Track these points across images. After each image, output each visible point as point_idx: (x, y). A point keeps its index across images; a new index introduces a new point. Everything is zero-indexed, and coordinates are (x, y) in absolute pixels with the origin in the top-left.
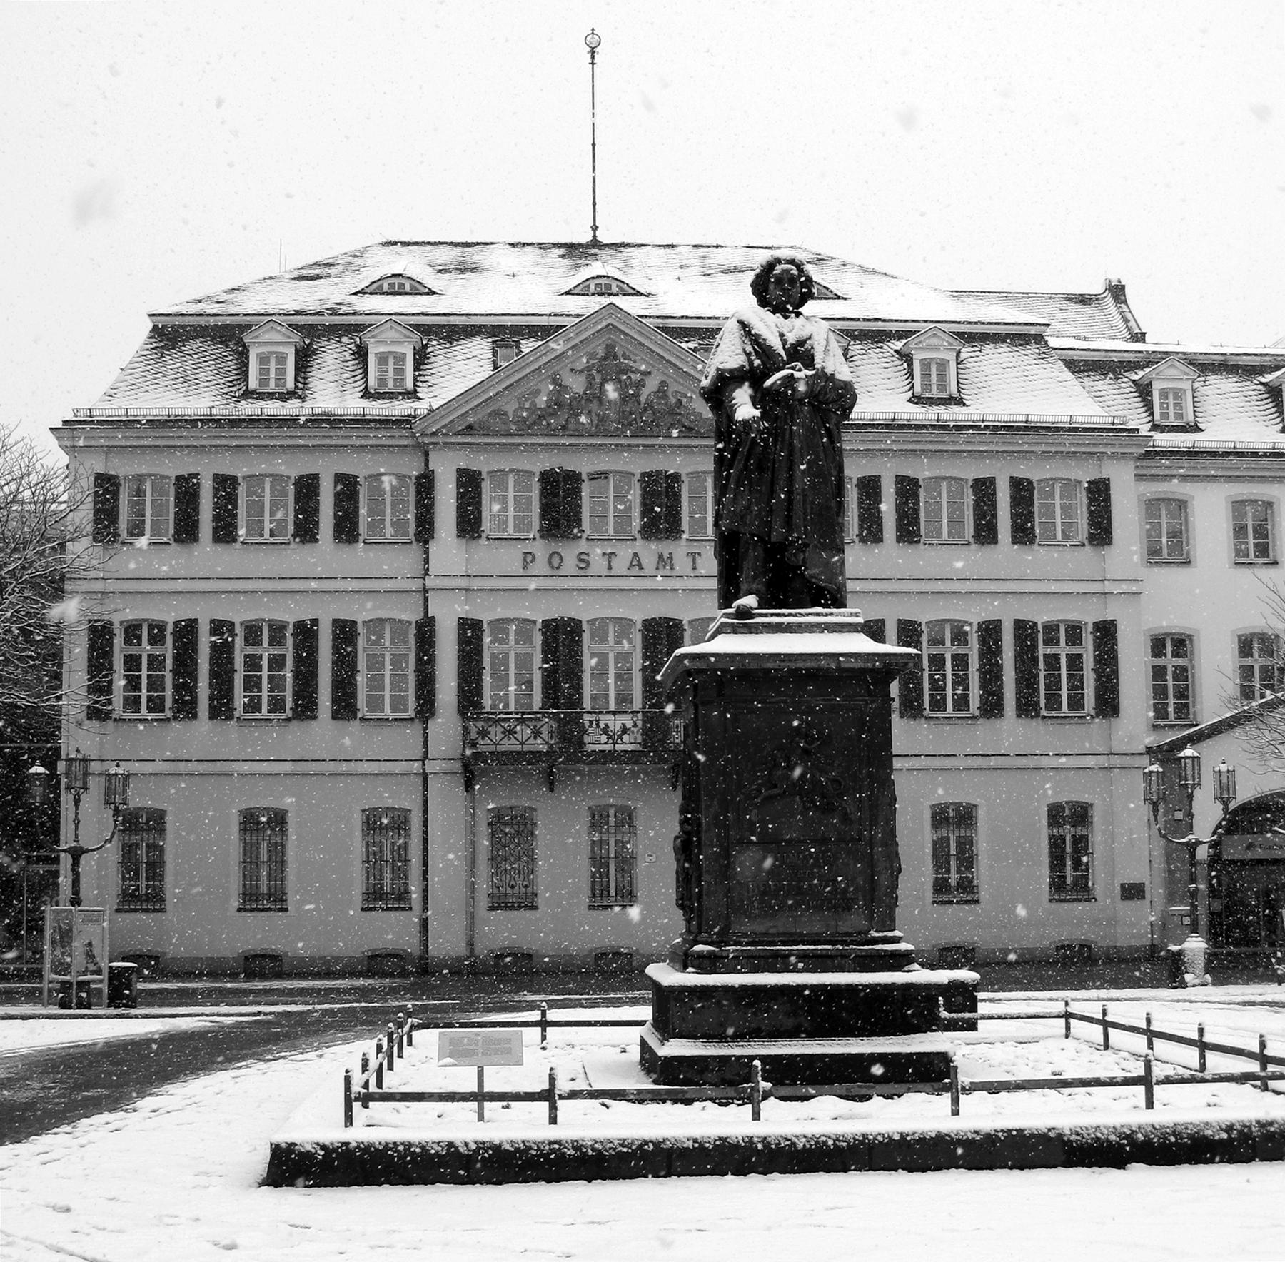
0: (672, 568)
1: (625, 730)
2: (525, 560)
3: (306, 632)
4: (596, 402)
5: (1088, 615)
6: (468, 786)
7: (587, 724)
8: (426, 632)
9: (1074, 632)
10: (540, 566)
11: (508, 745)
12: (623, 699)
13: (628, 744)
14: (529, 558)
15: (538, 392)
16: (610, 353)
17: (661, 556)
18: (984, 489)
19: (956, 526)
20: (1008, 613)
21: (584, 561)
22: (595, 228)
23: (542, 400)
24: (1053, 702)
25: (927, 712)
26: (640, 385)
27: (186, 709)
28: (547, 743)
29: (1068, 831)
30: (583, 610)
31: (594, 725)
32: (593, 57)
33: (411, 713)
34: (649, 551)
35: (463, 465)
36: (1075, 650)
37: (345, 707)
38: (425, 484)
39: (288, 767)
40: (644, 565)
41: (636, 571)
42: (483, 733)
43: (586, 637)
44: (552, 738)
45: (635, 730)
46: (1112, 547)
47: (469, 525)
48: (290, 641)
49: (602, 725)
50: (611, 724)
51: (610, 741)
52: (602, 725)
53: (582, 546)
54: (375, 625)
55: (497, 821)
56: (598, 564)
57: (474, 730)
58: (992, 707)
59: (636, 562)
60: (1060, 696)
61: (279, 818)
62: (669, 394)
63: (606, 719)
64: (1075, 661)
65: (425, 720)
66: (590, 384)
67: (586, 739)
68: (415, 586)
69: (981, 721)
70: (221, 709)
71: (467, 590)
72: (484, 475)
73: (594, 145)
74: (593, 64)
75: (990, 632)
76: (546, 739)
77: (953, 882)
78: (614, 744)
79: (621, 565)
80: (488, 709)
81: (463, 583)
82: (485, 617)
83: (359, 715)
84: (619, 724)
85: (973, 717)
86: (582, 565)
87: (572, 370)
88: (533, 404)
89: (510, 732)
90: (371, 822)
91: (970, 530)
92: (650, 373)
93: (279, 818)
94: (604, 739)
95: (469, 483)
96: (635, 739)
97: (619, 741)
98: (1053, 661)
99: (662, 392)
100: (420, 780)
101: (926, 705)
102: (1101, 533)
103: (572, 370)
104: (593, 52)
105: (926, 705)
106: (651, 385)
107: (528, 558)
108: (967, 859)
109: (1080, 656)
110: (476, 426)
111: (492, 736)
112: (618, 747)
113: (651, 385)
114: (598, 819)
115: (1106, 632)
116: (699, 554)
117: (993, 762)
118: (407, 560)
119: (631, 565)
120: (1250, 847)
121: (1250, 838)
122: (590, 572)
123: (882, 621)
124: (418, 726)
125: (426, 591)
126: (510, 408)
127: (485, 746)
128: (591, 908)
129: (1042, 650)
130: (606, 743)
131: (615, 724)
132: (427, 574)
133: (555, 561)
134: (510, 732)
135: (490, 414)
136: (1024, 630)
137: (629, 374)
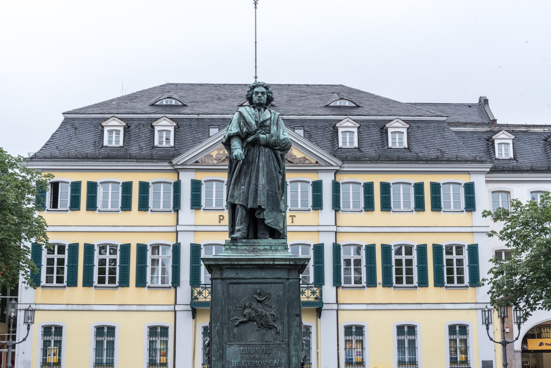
2: (220, 218)
3: (126, 249)
5: (466, 241)
6: (194, 317)
8: (176, 249)
9: (459, 249)
14: (222, 218)
18: (419, 188)
19: (407, 204)
20: (430, 241)
22: (256, 77)
24: (450, 280)
27: (72, 283)
29: (458, 338)
32: (256, 5)
33: (170, 285)
36: (459, 257)
37: (141, 282)
38: (177, 186)
39: (116, 308)
42: (200, 293)
46: (476, 212)
47: (196, 204)
48: (118, 252)
54: (156, 248)
57: (196, 292)
58: (423, 283)
60: (402, 277)
61: (111, 330)
64: (460, 262)
65: (176, 288)
68: (173, 229)
69: (418, 288)
70: (88, 282)
71: (195, 231)
72: (203, 182)
73: (256, 42)
74: (256, 8)
75: (422, 249)
77: (407, 360)
80: (203, 283)
81: (193, 228)
82: (202, 243)
83: (147, 285)
85: (416, 287)
90: (153, 331)
91: (413, 205)
93: (111, 330)
95: (196, 186)
98: (450, 262)
100: (173, 313)
101: (394, 280)
102: (470, 205)
104: (256, 4)
109: (462, 260)
111: (204, 294)
115: (473, 250)
116: (295, 216)
117: (424, 307)
118: (170, 218)
120: (541, 344)
121: (540, 340)
123: (375, 245)
124: (173, 290)
125: (177, 232)
129: (445, 257)
132: (177, 224)
136: (437, 249)
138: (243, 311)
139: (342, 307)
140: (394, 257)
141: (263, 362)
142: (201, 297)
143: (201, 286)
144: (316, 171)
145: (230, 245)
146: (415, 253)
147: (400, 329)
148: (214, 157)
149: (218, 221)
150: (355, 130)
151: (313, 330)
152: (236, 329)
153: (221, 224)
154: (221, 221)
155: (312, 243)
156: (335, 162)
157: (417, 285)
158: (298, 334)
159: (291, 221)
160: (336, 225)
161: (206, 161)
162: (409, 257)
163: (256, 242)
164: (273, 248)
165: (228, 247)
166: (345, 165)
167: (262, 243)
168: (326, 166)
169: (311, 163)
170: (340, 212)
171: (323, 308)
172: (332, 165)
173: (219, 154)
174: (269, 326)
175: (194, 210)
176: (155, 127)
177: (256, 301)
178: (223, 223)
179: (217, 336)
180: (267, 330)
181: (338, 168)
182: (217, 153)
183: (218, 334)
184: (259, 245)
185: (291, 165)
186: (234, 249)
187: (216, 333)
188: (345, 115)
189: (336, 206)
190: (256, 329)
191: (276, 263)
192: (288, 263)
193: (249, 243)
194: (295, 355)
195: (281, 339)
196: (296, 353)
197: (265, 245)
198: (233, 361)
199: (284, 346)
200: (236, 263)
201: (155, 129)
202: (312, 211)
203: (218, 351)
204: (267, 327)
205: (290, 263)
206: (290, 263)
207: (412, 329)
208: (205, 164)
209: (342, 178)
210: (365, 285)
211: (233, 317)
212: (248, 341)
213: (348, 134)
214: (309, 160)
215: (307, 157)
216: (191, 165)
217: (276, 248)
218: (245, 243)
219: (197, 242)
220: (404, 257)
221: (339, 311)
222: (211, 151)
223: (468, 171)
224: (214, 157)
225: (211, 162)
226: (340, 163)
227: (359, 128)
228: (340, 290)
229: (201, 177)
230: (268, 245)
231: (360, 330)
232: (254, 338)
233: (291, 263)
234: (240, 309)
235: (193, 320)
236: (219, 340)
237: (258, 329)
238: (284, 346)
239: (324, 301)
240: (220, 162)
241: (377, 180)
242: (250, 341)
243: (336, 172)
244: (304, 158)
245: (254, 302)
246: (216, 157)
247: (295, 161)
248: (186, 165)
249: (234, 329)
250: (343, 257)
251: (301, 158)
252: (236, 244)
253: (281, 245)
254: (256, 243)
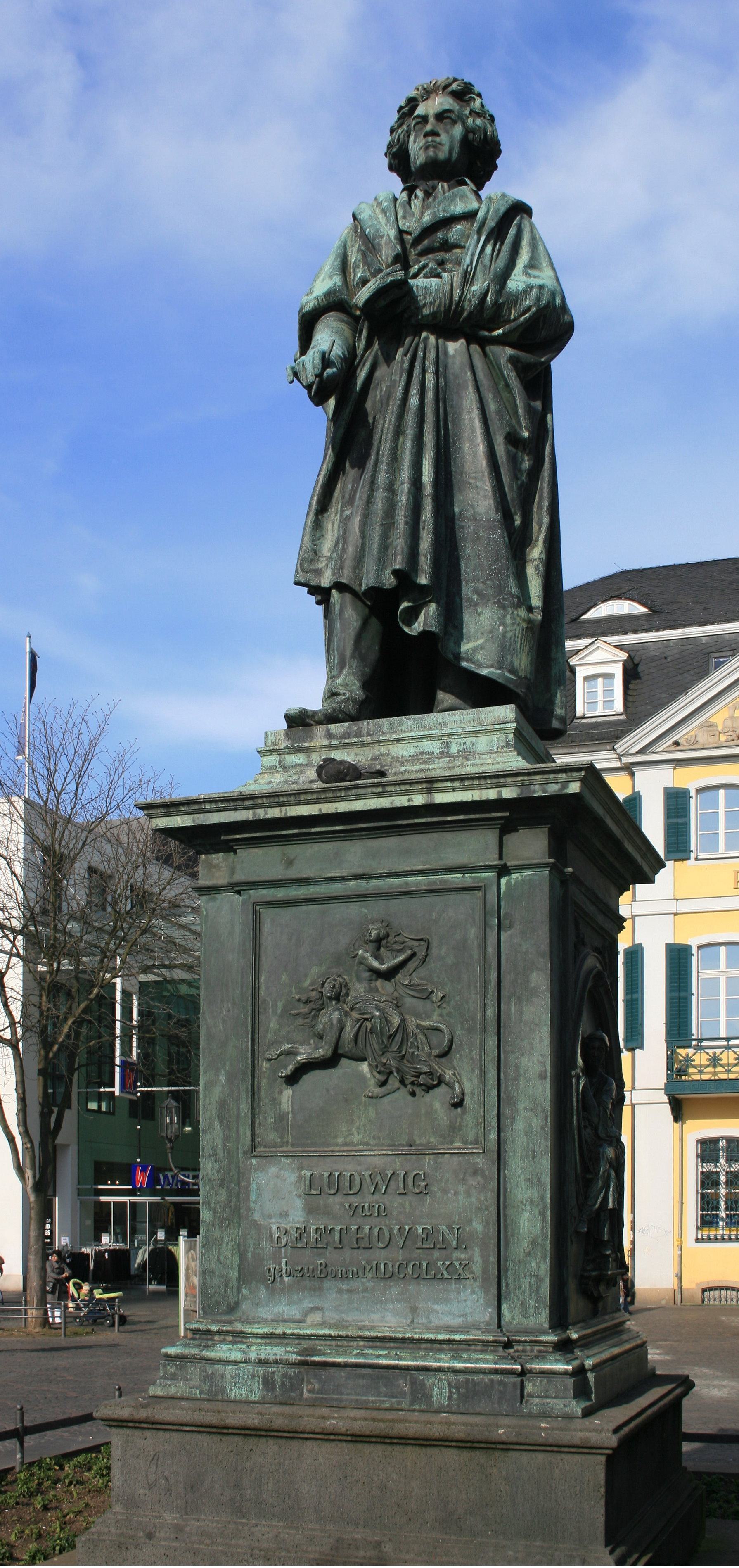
138: (315, 1017)
141: (391, 1230)
145: (279, 752)
148: (720, 728)
152: (288, 1092)
158: (544, 1110)
163: (385, 729)
164: (454, 749)
165: (273, 760)
167: (412, 731)
174: (418, 1077)
176: (578, 669)
177: (367, 974)
179: (217, 1125)
180: (413, 1094)
182: (727, 716)
183: (220, 1117)
184: (398, 741)
186: (296, 765)
187: (215, 1112)
190: (367, 1092)
191: (440, 798)
192: (491, 794)
193: (358, 734)
194: (532, 1202)
195: (471, 1135)
196: (536, 1194)
197: (421, 738)
198: (274, 1228)
199: (480, 1161)
200: (274, 813)
201: (578, 675)
203: (221, 1185)
204: (412, 1083)
205: (499, 793)
206: (499, 793)
211: (277, 1043)
212: (337, 1145)
216: (663, 752)
217: (469, 746)
218: (346, 735)
225: (711, 739)
230: (432, 738)
232: (358, 1128)
233: (508, 793)
234: (304, 1009)
236: (226, 1139)
237: (378, 1091)
238: (480, 1161)
242: (346, 1144)
245: (359, 979)
246: (724, 728)
249: (281, 1092)
252: (306, 745)
253: (486, 732)
254: (384, 733)
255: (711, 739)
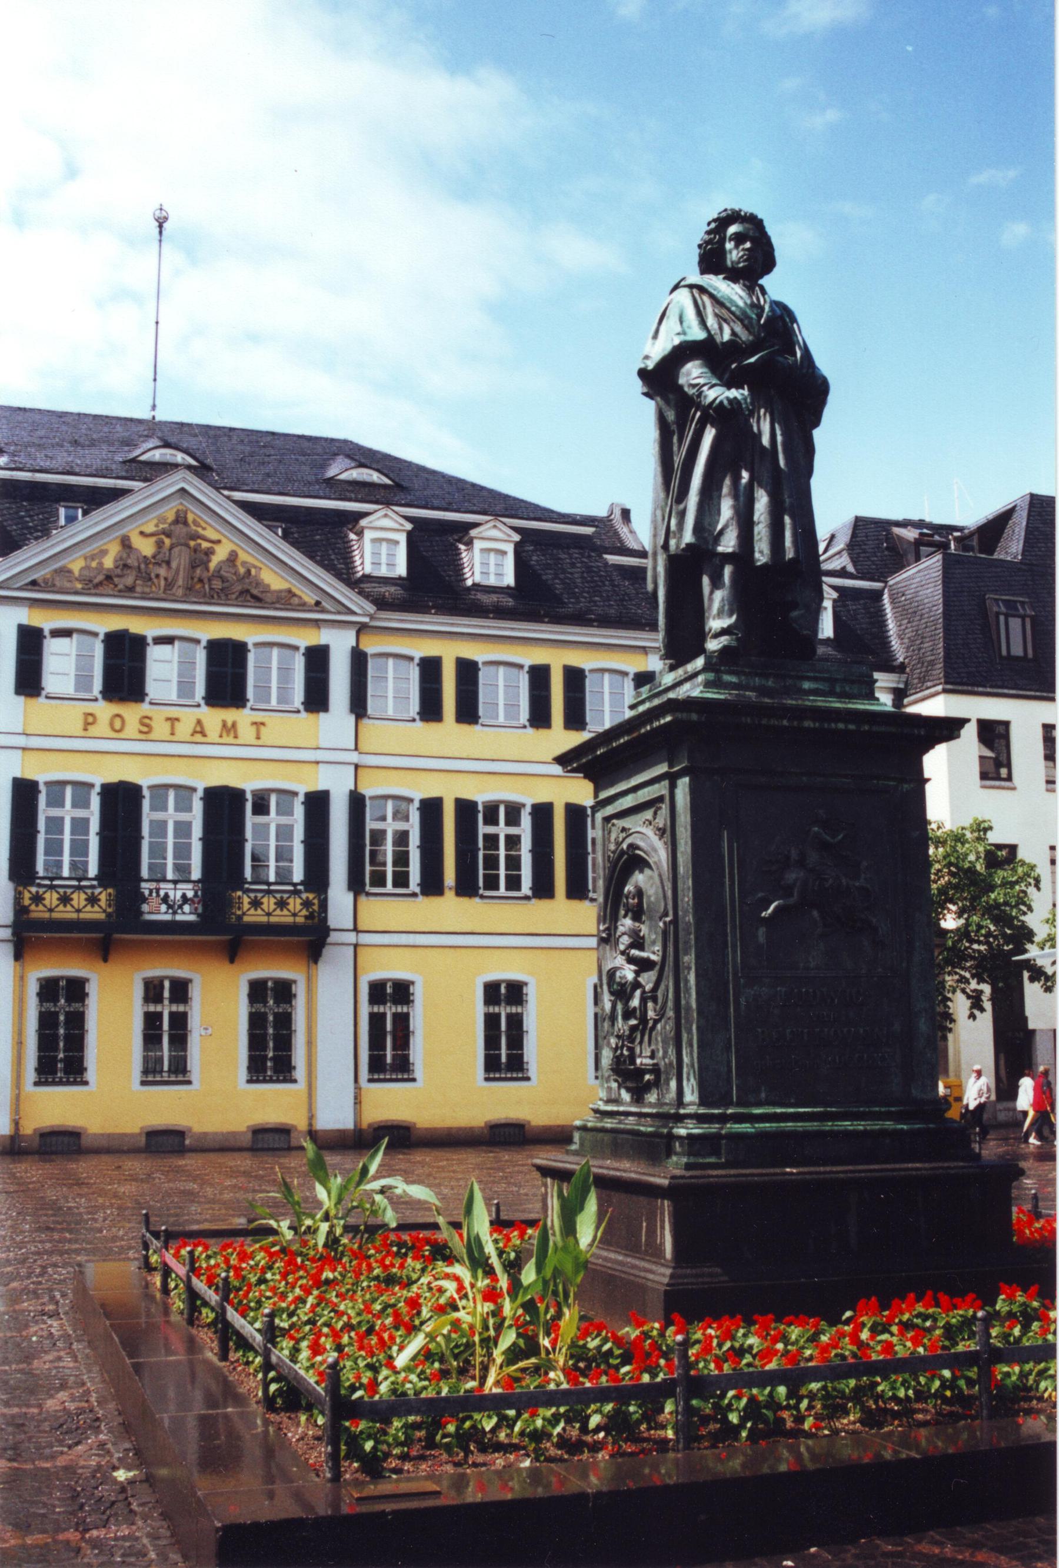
0: (236, 737)
1: (185, 899)
2: (86, 719)
4: (164, 565)
6: (18, 956)
7: (147, 893)
10: (102, 728)
11: (65, 913)
12: (183, 870)
13: (187, 915)
15: (104, 553)
16: (180, 519)
17: (224, 724)
21: (146, 724)
22: (154, 407)
23: (109, 562)
25: (481, 892)
26: (209, 553)
28: (105, 911)
30: (142, 774)
31: (154, 894)
34: (214, 718)
35: (25, 621)
40: (208, 733)
41: (199, 738)
42: (37, 899)
43: (146, 804)
44: (110, 906)
45: (196, 900)
49: (162, 893)
50: (171, 894)
51: (170, 911)
52: (162, 893)
53: (145, 708)
55: (48, 989)
56: (161, 729)
57: (27, 895)
59: (200, 729)
62: (238, 563)
63: (165, 888)
66: (160, 544)
67: (145, 908)
69: (534, 901)
71: (24, 749)
76: (104, 906)
78: (175, 913)
79: (184, 729)
81: (21, 741)
82: (41, 777)
84: (179, 894)
85: (527, 898)
86: (145, 729)
87: (142, 533)
88: (101, 564)
89: (65, 900)
92: (219, 542)
94: (164, 908)
96: (196, 909)
97: (179, 911)
99: (233, 557)
101: (481, 884)
103: (142, 533)
105: (481, 884)
106: (221, 554)
107: (89, 720)
108: (517, 1038)
110: (40, 581)
112: (179, 918)
113: (221, 554)
114: (152, 991)
116: (263, 724)
119: (195, 732)
122: (152, 736)
126: (77, 566)
127: (38, 912)
128: (144, 1083)
130: (166, 913)
131: (176, 895)
133: (117, 726)
134: (65, 900)
135: (56, 571)
137: (199, 541)
139: (365, 939)
140: (483, 829)
142: (41, 907)
143: (38, 881)
144: (317, 623)
146: (526, 821)
147: (492, 992)
148: (77, 573)
149: (80, 724)
150: (402, 538)
151: (300, 990)
153: (89, 734)
154: (89, 727)
155: (302, 789)
156: (361, 608)
157: (529, 893)
159: (255, 735)
160: (356, 749)
161: (58, 584)
162: (513, 831)
166: (383, 615)
168: (339, 613)
169: (304, 604)
170: (365, 721)
171: (330, 940)
172: (353, 613)
173: (87, 567)
175: (22, 698)
178: (93, 731)
181: (366, 620)
185: (257, 604)
188: (376, 502)
189: (359, 706)
202: (304, 715)
207: (515, 992)
208: (55, 589)
209: (372, 646)
210: (418, 890)
213: (384, 545)
214: (300, 598)
215: (294, 590)
216: (20, 589)
219: (30, 775)
220: (502, 830)
221: (359, 949)
222: (70, 559)
223: (644, 648)
224: (77, 573)
226: (371, 608)
227: (410, 535)
228: (363, 899)
229: (46, 621)
231: (402, 992)
235: (17, 964)
239: (332, 923)
240: (90, 586)
241: (449, 653)
243: (361, 629)
244: (289, 591)
246: (80, 575)
247: (269, 598)
248: (9, 589)
250: (370, 825)
251: (281, 591)
255: (68, 585)
